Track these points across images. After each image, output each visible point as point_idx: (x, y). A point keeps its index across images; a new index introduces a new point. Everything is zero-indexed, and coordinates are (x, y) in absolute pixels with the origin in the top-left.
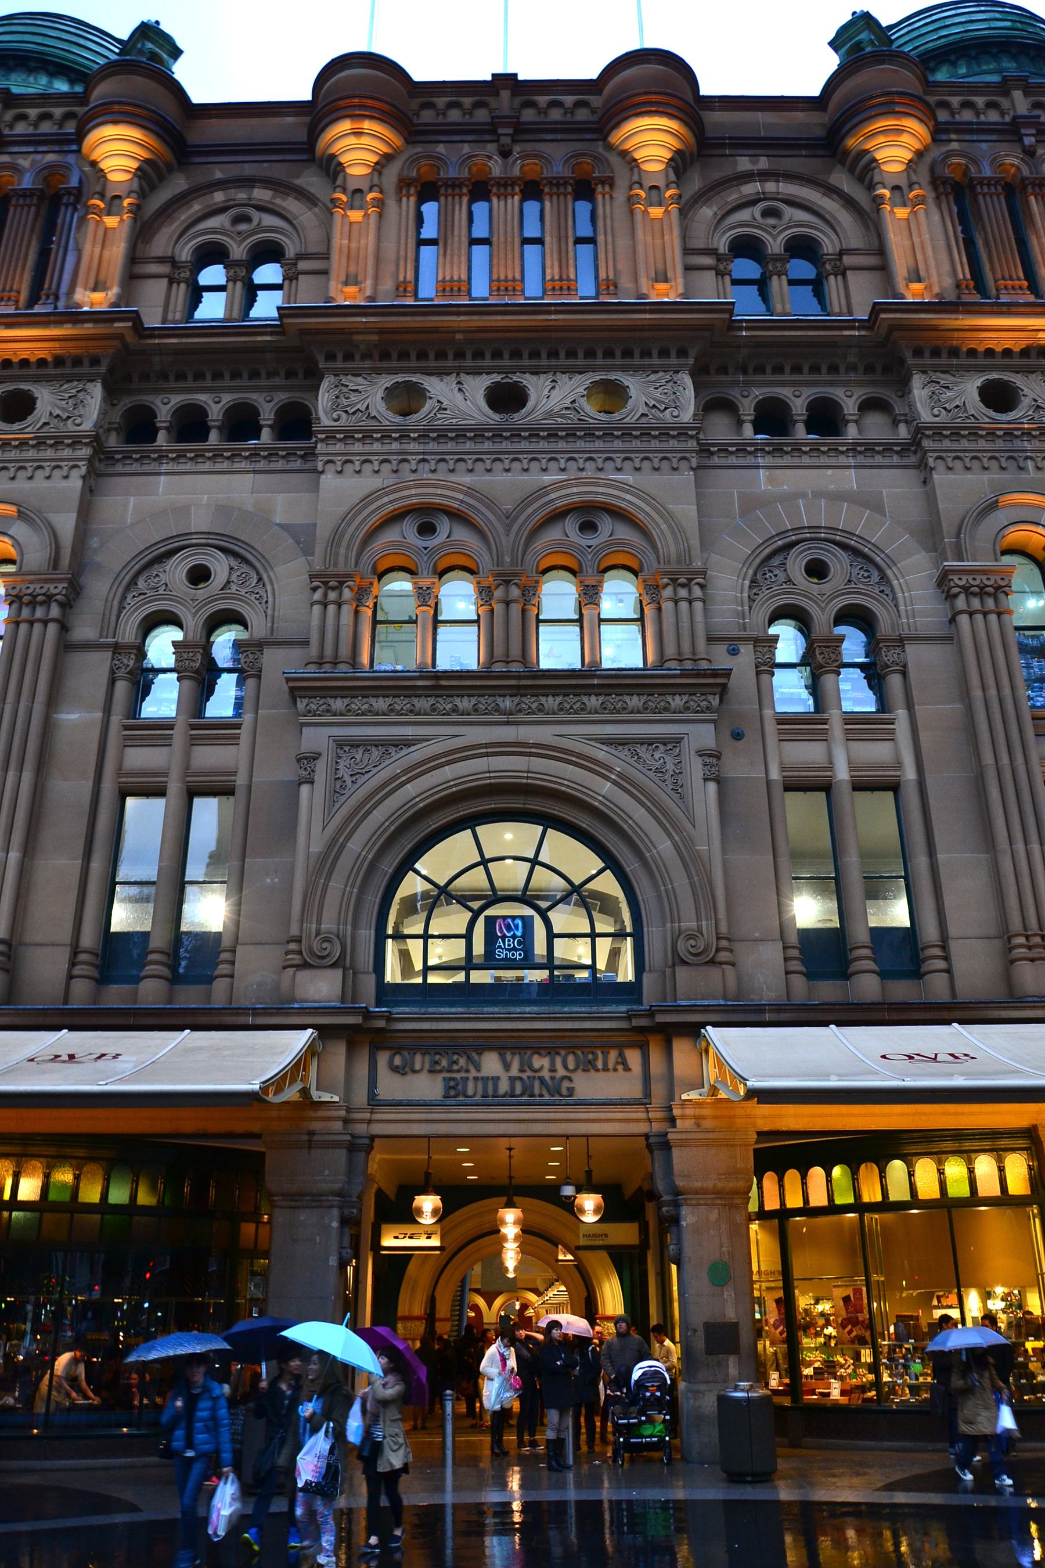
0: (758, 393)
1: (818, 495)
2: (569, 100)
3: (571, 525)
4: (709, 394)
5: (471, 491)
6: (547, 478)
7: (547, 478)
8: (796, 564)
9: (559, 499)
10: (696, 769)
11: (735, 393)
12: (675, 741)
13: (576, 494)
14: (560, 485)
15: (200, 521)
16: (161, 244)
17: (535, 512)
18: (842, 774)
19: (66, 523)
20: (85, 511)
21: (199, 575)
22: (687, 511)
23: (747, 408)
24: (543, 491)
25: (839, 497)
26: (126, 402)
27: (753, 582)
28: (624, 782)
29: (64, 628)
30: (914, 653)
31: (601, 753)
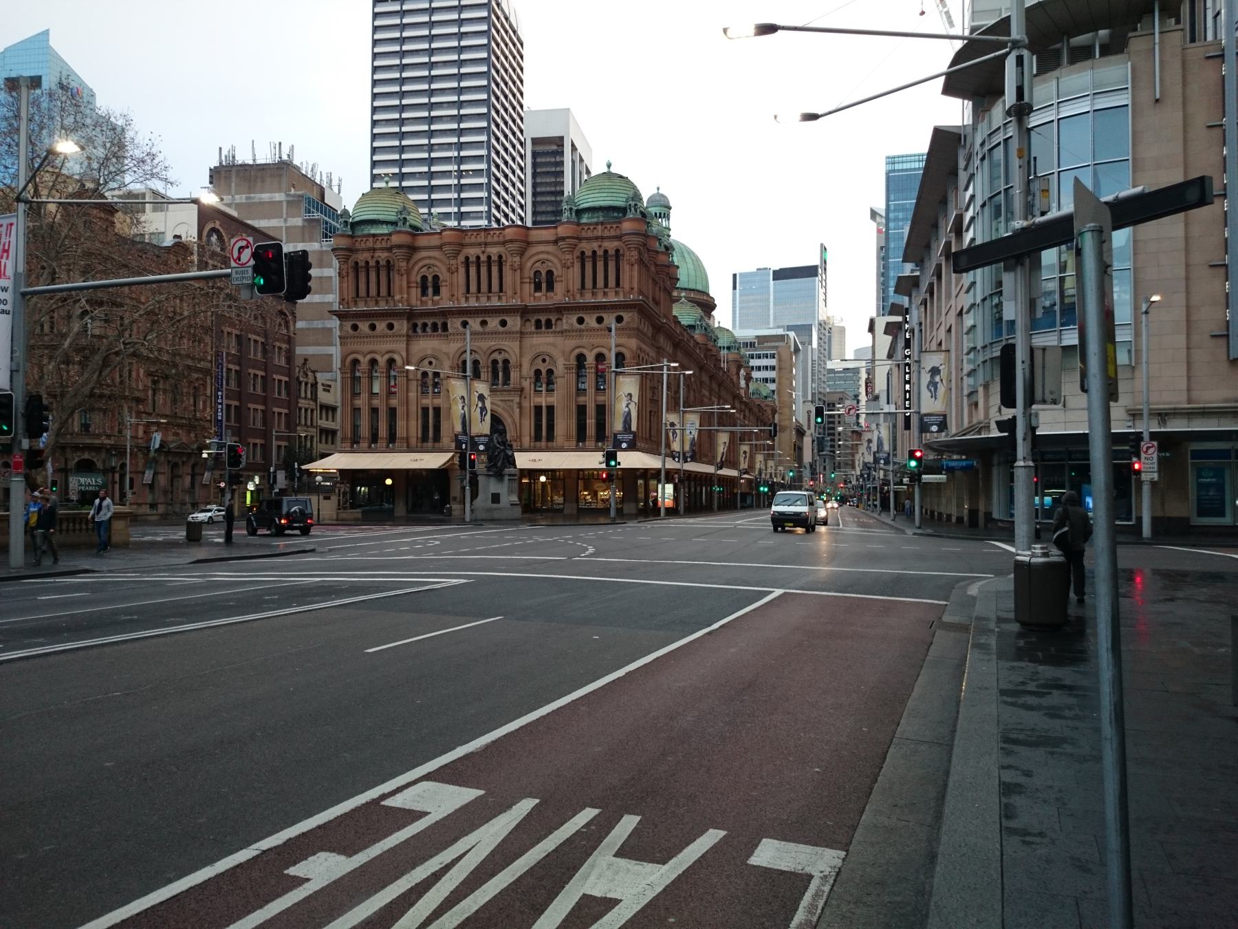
0: (536, 318)
1: (545, 344)
2: (498, 232)
3: (497, 352)
4: (525, 319)
5: (478, 347)
6: (493, 343)
7: (493, 343)
8: (540, 359)
9: (494, 348)
10: (516, 406)
11: (530, 318)
12: (512, 401)
13: (497, 347)
14: (495, 345)
15: (429, 352)
16: (413, 278)
17: (489, 352)
18: (544, 405)
19: (404, 354)
20: (408, 350)
21: (430, 363)
22: (517, 351)
23: (533, 322)
24: (490, 347)
25: (549, 344)
26: (412, 322)
27: (531, 364)
28: (503, 409)
29: (407, 377)
30: (558, 379)
31: (500, 403)
